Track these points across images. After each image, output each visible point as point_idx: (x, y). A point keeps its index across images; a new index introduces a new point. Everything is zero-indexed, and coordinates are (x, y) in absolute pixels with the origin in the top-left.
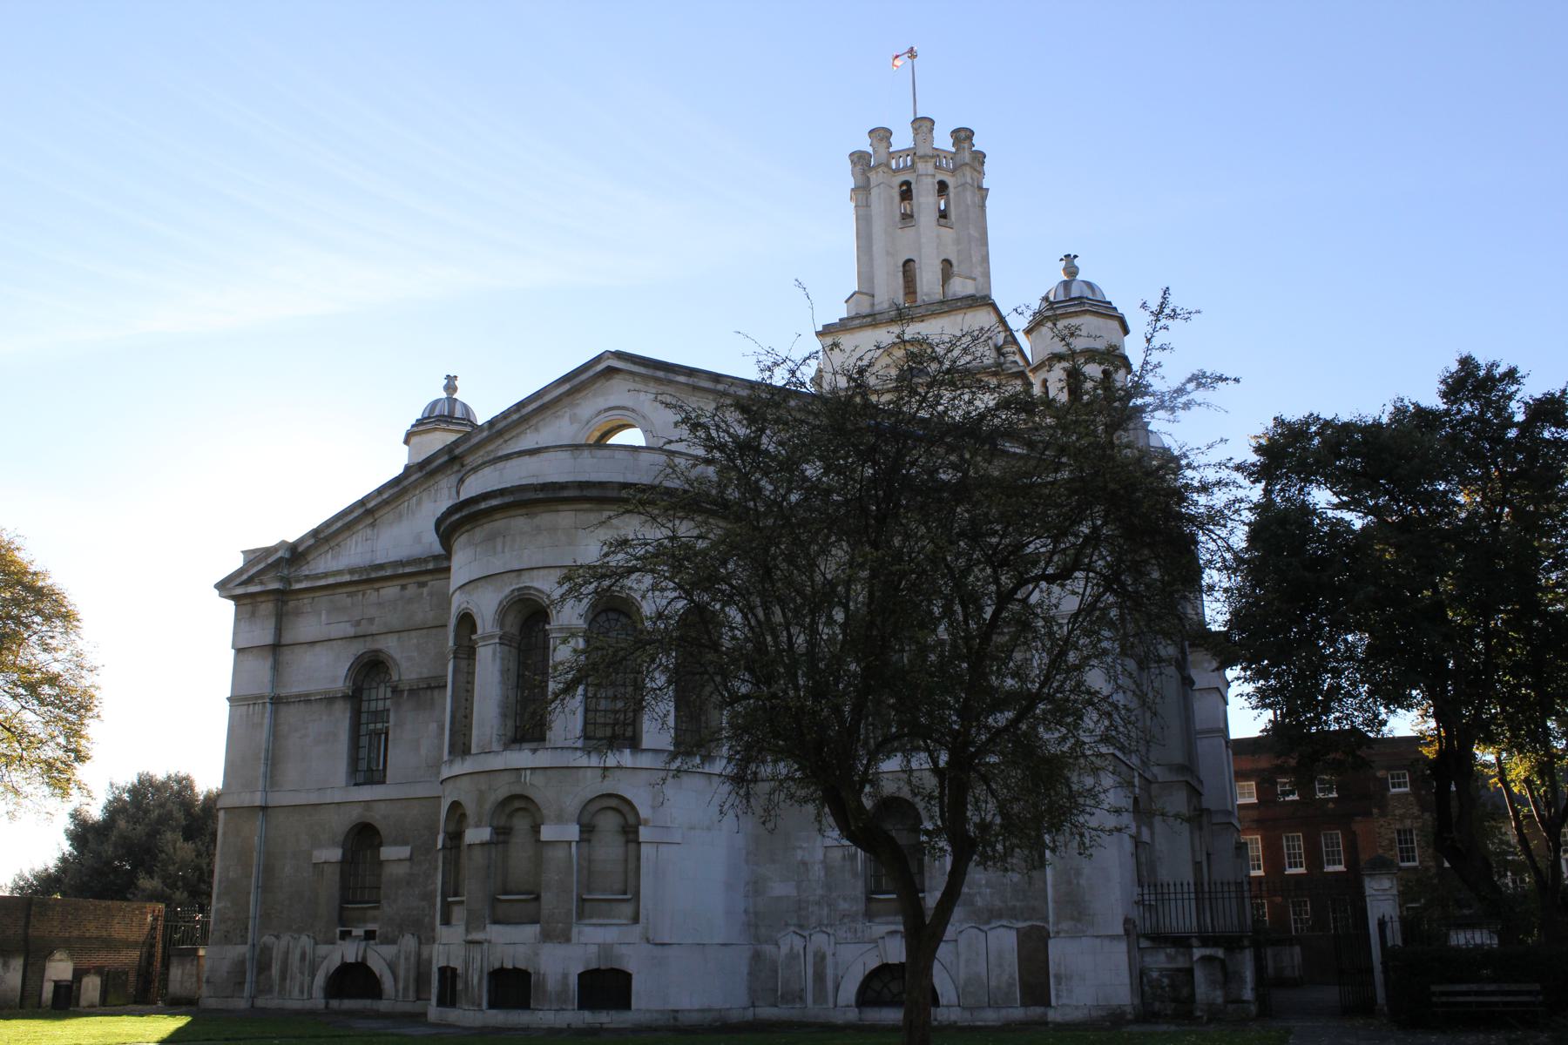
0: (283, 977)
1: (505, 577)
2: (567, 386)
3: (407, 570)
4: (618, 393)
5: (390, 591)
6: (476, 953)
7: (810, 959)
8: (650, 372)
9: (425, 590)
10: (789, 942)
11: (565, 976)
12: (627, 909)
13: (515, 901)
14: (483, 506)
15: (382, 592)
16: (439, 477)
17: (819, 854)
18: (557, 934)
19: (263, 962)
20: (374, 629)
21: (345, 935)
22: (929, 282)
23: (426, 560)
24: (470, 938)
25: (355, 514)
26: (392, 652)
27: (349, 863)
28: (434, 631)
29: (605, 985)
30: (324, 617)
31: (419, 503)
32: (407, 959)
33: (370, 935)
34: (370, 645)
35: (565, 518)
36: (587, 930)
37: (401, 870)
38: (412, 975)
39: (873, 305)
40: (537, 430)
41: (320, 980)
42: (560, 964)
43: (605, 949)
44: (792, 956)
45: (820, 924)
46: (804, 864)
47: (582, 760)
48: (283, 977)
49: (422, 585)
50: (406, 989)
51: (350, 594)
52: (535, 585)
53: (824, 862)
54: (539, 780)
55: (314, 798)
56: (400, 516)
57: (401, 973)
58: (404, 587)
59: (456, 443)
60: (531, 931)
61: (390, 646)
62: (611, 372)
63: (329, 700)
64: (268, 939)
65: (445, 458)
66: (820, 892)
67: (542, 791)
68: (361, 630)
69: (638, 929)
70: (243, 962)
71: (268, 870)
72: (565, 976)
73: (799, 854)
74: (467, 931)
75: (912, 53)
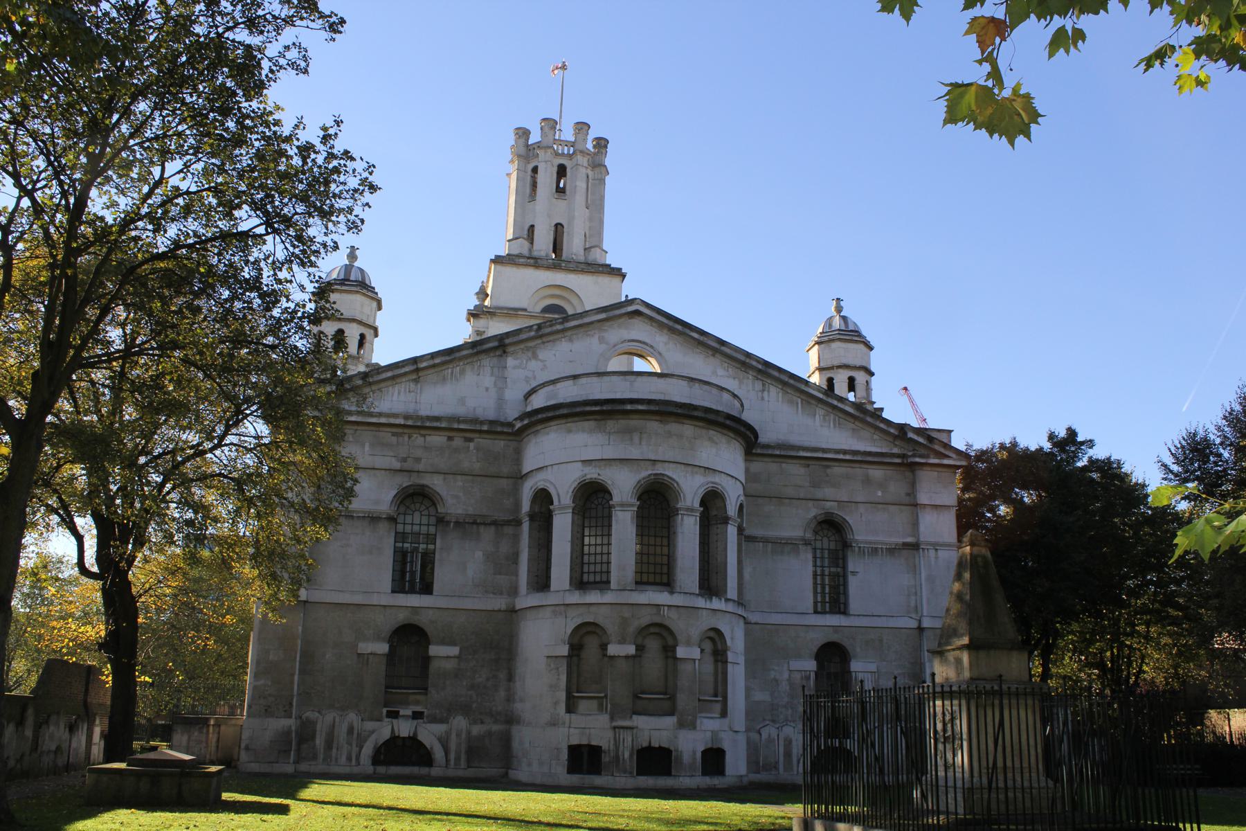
0: (329, 744)
1: (642, 463)
2: (603, 316)
3: (462, 426)
4: (639, 331)
5: (437, 439)
6: (627, 738)
7: (782, 743)
8: (671, 324)
9: (472, 445)
10: (769, 731)
11: (694, 752)
12: (718, 707)
13: (663, 700)
14: (629, 407)
15: (428, 438)
16: (482, 356)
17: (786, 675)
18: (687, 724)
19: (305, 733)
20: (421, 467)
21: (394, 715)
22: (574, 246)
23: (482, 423)
24: (615, 724)
25: (407, 369)
26: (438, 489)
28: (479, 479)
30: (367, 448)
31: (462, 372)
32: (458, 735)
33: (417, 716)
34: (416, 480)
35: (688, 429)
36: (705, 721)
37: (449, 665)
38: (463, 748)
39: (530, 250)
40: (571, 340)
43: (715, 734)
44: (770, 740)
45: (787, 720)
46: (777, 681)
47: (701, 602)
48: (329, 744)
49: (471, 440)
50: (458, 759)
51: (394, 434)
52: (670, 474)
53: (789, 680)
54: (673, 614)
55: (358, 599)
56: (444, 379)
57: (453, 747)
58: (450, 439)
59: (508, 334)
60: (670, 721)
61: (436, 483)
62: (637, 313)
63: (373, 519)
64: (310, 714)
65: (496, 344)
66: (786, 700)
67: (676, 622)
68: (407, 466)
69: (726, 721)
70: (289, 733)
71: (308, 657)
72: (694, 752)
73: (773, 674)
74: (612, 719)
75: (564, 67)
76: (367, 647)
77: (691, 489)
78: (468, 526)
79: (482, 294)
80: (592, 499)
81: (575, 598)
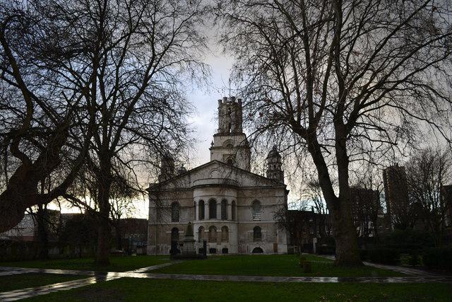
27: (172, 234)
29: (225, 250)
41: (169, 251)
42: (220, 248)
43: (225, 246)
60: (216, 244)
76: (167, 232)
77: (219, 200)
78: (185, 208)
79: (212, 144)
80: (202, 203)
81: (199, 222)
